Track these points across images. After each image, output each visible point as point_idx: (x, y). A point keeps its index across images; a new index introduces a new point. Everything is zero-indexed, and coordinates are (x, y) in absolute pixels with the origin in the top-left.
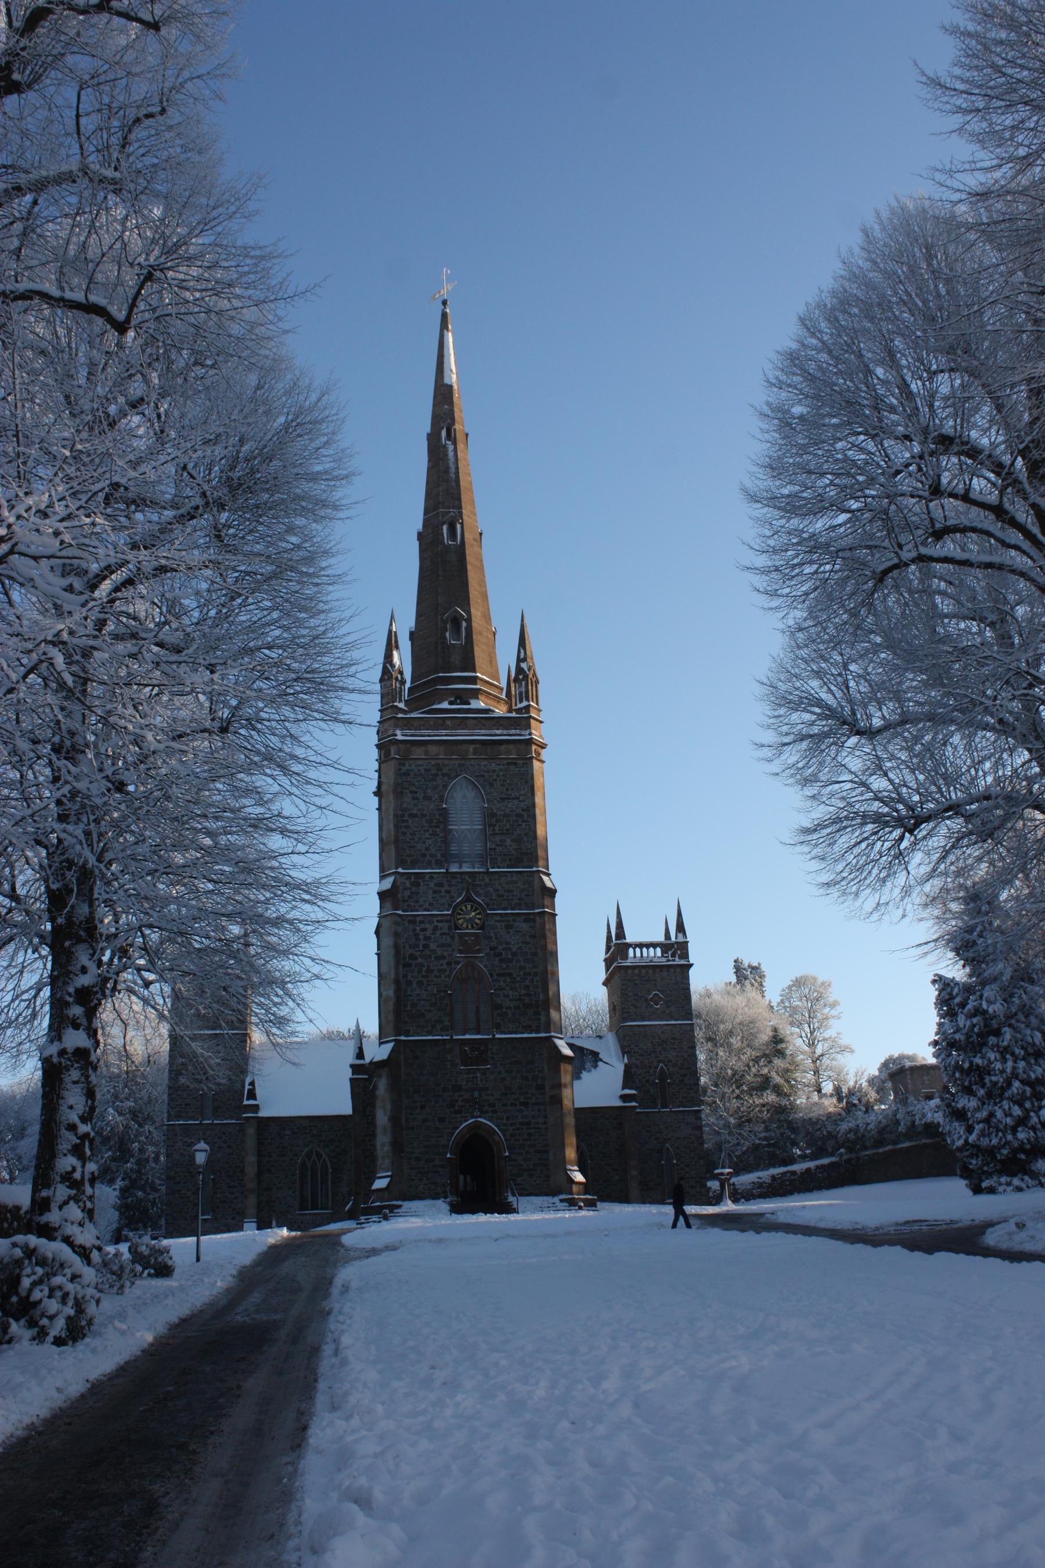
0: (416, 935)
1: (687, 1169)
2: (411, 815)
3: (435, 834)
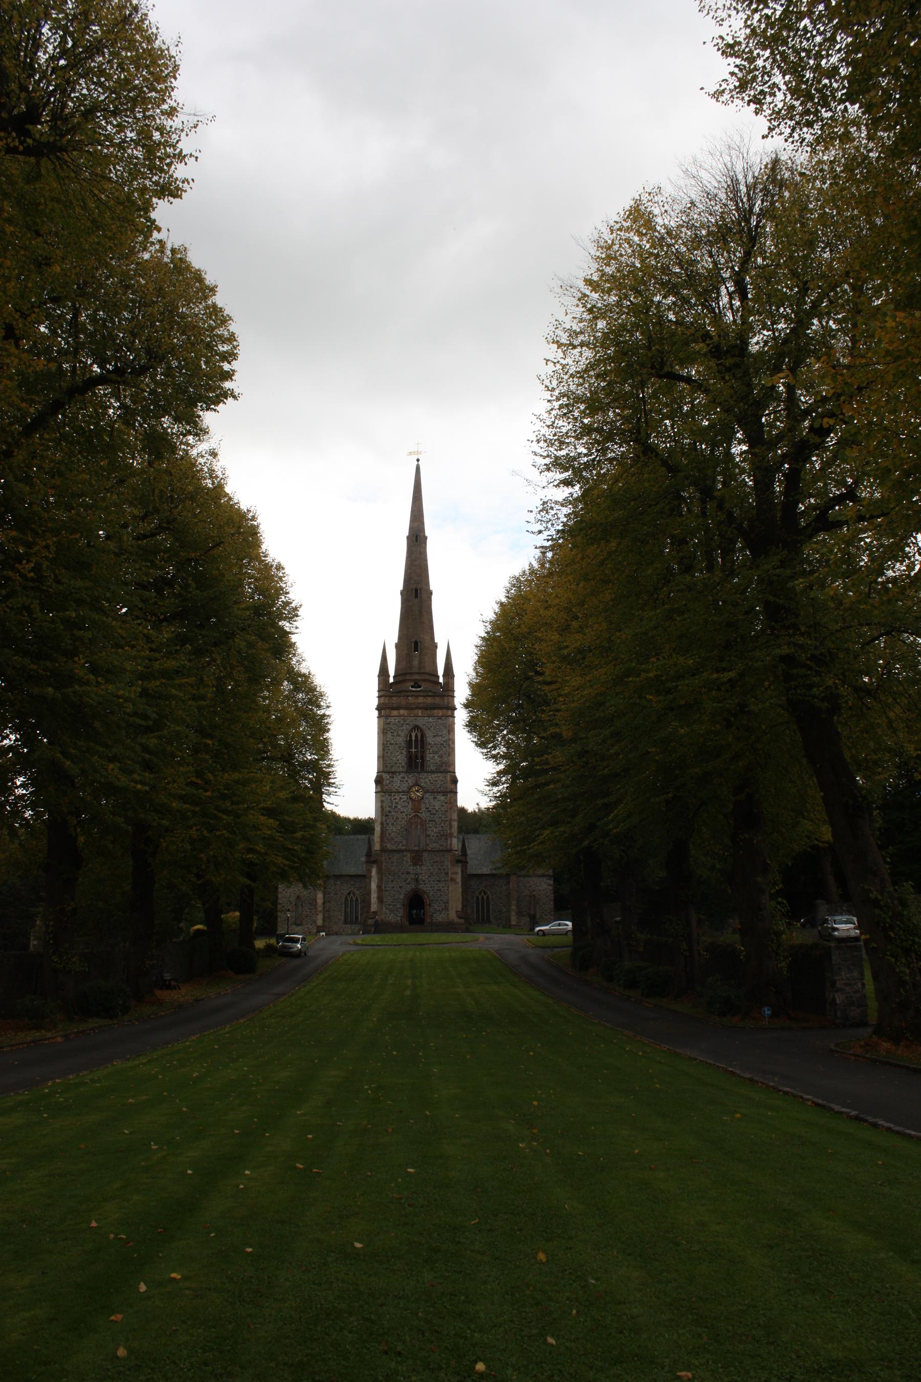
0: (392, 802)
2: (391, 744)
3: (401, 753)
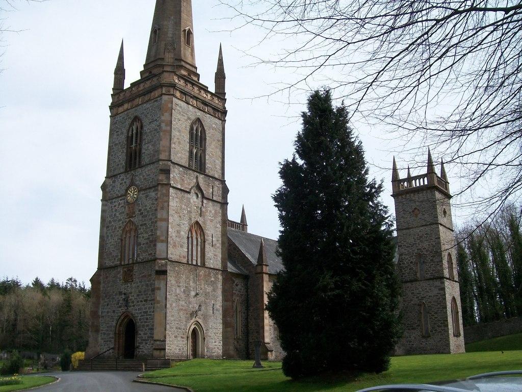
1: (436, 316)
